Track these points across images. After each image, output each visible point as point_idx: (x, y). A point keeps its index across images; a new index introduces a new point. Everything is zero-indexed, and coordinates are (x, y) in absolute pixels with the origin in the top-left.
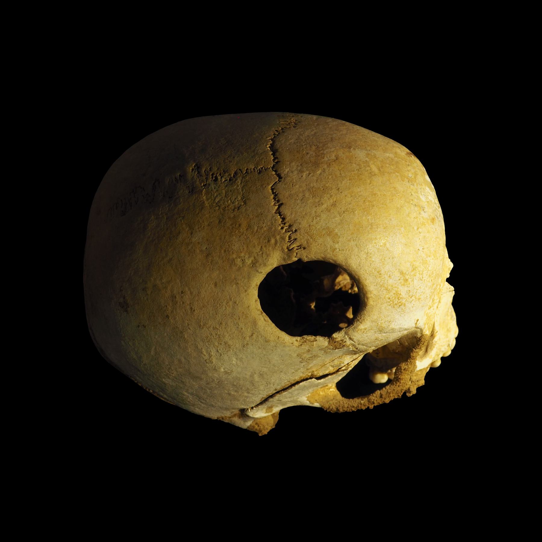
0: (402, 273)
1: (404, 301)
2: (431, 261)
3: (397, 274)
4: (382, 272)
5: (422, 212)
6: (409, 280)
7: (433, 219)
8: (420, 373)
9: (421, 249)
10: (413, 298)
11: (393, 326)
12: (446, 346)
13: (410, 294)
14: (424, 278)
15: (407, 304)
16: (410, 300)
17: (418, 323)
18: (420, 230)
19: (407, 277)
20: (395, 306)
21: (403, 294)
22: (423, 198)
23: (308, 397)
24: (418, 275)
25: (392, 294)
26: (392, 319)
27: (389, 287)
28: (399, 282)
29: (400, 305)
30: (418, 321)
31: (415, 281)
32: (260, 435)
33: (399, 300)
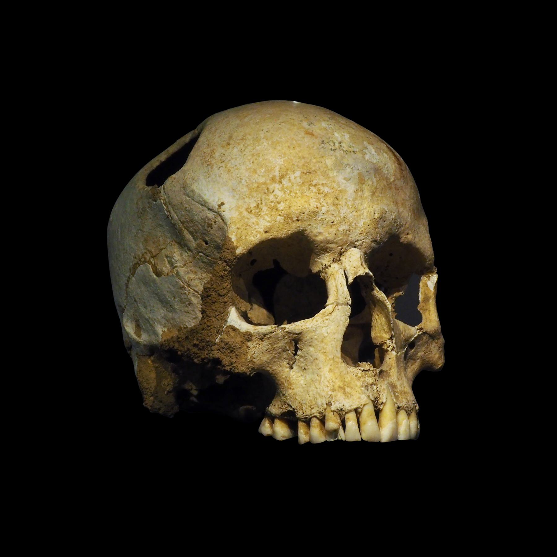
0: (230, 137)
1: (213, 162)
2: (265, 144)
3: (226, 137)
4: (218, 131)
5: (305, 124)
6: (231, 146)
7: (312, 134)
8: (233, 334)
9: (265, 131)
10: (223, 164)
11: (195, 187)
12: (325, 402)
13: (223, 158)
14: (245, 153)
15: (214, 167)
16: (220, 165)
17: (223, 207)
18: (283, 124)
19: (231, 142)
20: (205, 164)
21: (217, 155)
22: (324, 124)
23: (163, 332)
24: (242, 146)
25: (209, 150)
26: (196, 178)
27: (212, 144)
28: (222, 142)
29: (210, 165)
30: (223, 204)
31: (235, 150)
32: (144, 404)
33: (210, 158)
